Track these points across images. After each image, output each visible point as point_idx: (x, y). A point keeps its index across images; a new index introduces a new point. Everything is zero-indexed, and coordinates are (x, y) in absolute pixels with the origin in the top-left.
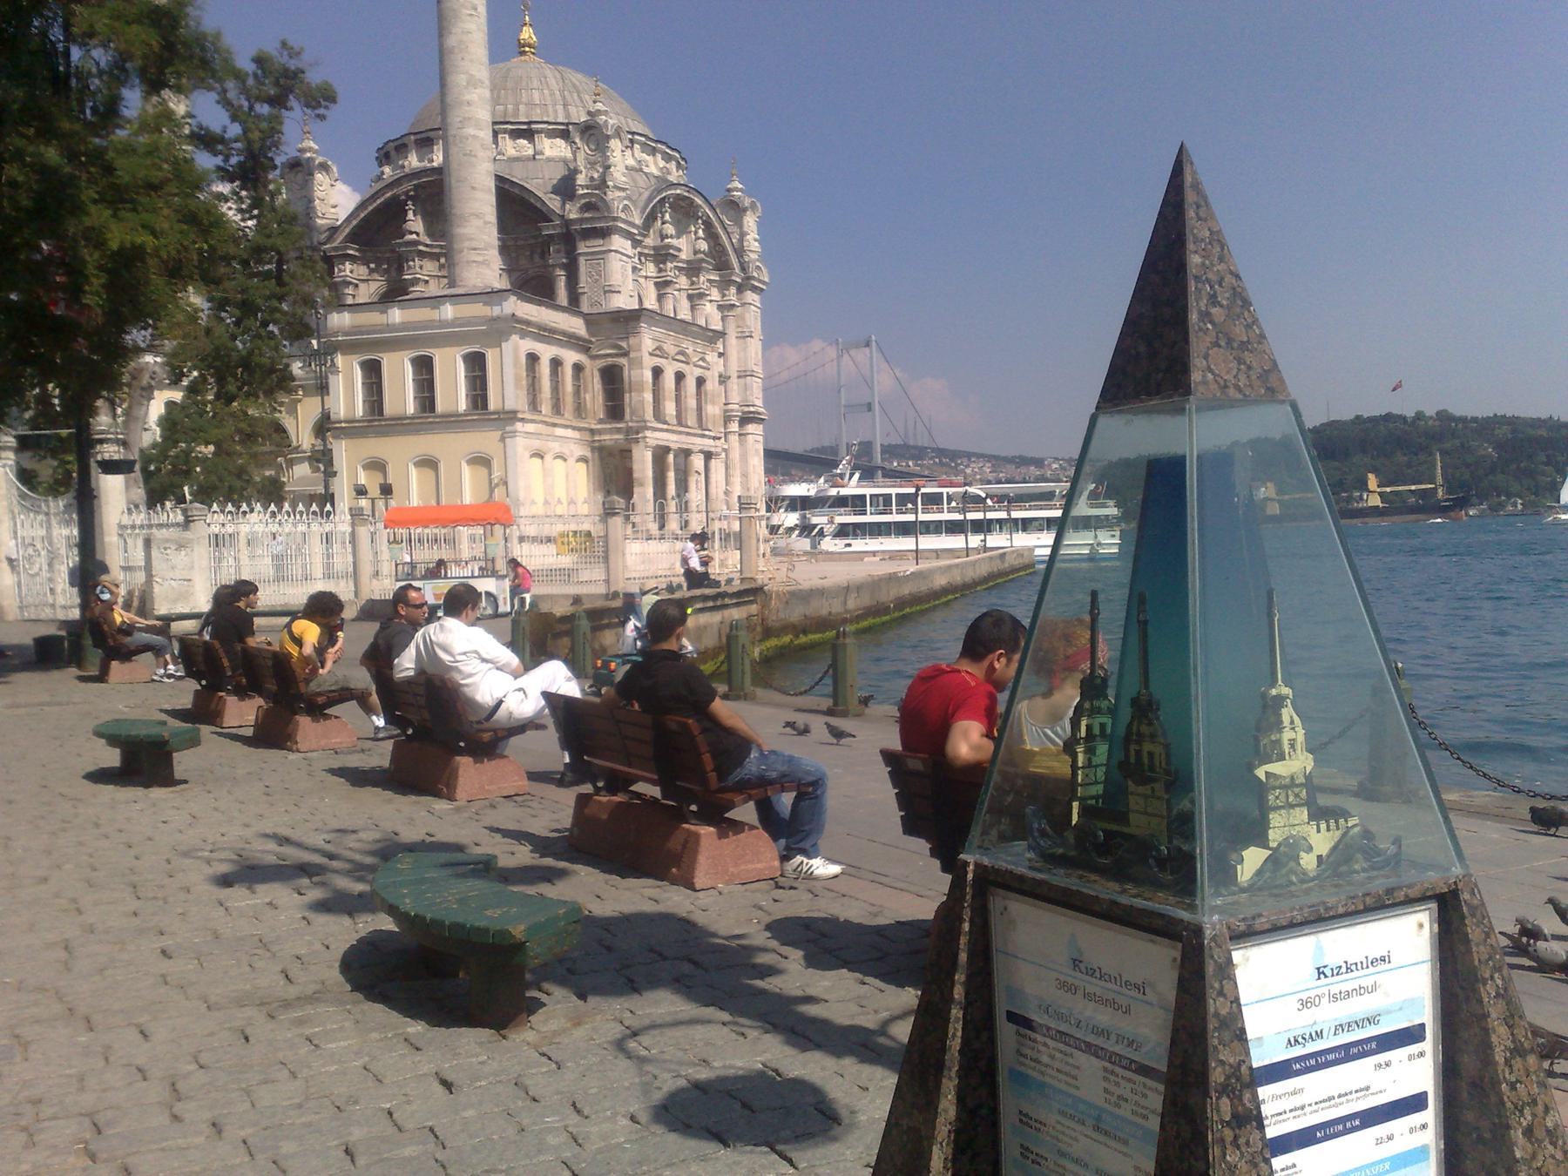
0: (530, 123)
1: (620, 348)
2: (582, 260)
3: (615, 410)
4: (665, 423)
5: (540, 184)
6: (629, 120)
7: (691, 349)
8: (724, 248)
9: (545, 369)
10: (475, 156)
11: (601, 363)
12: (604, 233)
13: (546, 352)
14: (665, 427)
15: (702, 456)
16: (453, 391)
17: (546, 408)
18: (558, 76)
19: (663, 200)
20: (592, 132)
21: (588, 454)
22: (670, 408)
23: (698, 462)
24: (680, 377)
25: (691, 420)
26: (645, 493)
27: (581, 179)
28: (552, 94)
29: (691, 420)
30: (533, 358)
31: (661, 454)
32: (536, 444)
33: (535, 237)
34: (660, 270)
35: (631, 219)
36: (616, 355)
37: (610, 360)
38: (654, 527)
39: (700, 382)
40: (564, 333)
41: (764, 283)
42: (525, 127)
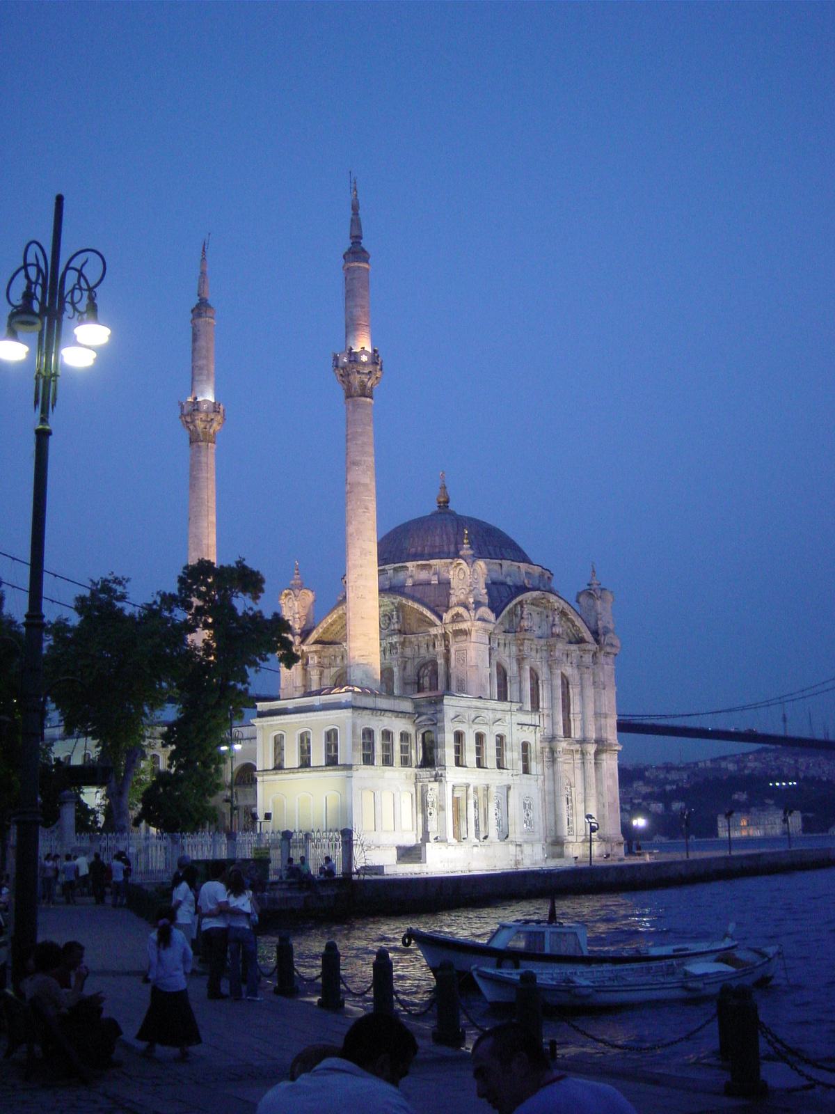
2: (452, 651)
4: (466, 767)
10: (364, 598)
17: (378, 759)
19: (521, 603)
20: (461, 567)
22: (470, 757)
24: (480, 738)
28: (449, 539)
30: (368, 733)
34: (520, 650)
39: (500, 739)
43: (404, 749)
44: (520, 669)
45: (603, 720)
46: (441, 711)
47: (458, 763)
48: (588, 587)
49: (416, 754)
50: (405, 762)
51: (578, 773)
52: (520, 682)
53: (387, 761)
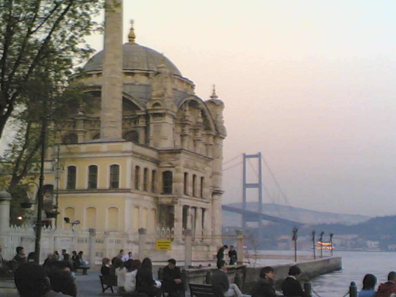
0: (133, 70)
2: (152, 126)
3: (167, 189)
5: (136, 95)
9: (142, 173)
13: (143, 165)
16: (104, 180)
19: (185, 102)
21: (155, 207)
22: (190, 190)
23: (199, 212)
24: (194, 176)
25: (198, 194)
26: (178, 226)
27: (154, 94)
29: (198, 194)
30: (137, 167)
31: (185, 208)
33: (133, 115)
34: (183, 130)
39: (202, 178)
47: (185, 193)
48: (210, 99)
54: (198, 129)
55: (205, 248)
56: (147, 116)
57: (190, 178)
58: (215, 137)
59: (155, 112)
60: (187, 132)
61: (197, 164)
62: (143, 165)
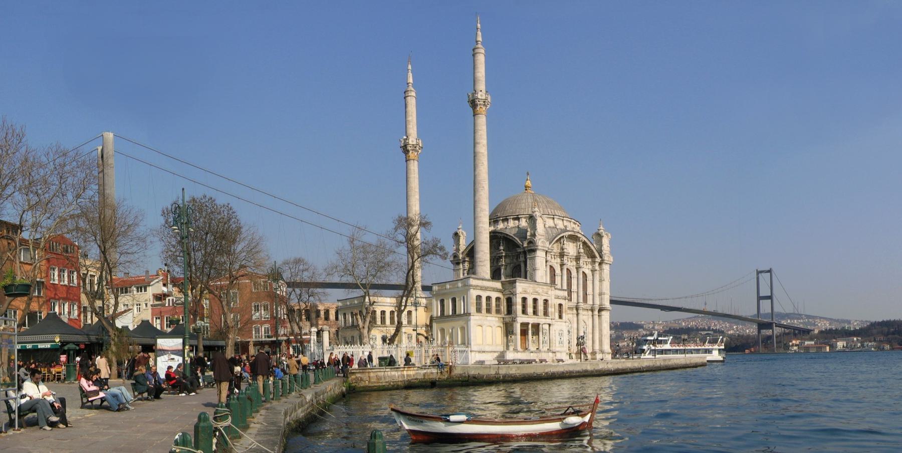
0: (518, 215)
1: (511, 292)
2: (528, 260)
3: (510, 310)
4: (528, 315)
6: (556, 211)
7: (541, 291)
8: (592, 251)
11: (506, 297)
12: (534, 251)
13: (484, 294)
14: (527, 316)
15: (548, 325)
18: (532, 197)
19: (563, 237)
21: (502, 325)
22: (530, 310)
24: (535, 300)
27: (528, 234)
32: (479, 323)
34: (562, 260)
35: (545, 246)
36: (510, 294)
37: (508, 296)
38: (519, 348)
39: (546, 301)
40: (491, 288)
41: (611, 261)
42: (515, 217)
43: (498, 306)
44: (562, 270)
45: (603, 296)
46: (515, 287)
47: (524, 312)
49: (504, 307)
50: (498, 311)
51: (591, 320)
52: (562, 276)
53: (489, 311)
54: (580, 258)
55: (551, 354)
56: (525, 253)
57: (530, 302)
58: (600, 264)
59: (529, 248)
60: (565, 262)
61: (537, 290)
62: (484, 294)
